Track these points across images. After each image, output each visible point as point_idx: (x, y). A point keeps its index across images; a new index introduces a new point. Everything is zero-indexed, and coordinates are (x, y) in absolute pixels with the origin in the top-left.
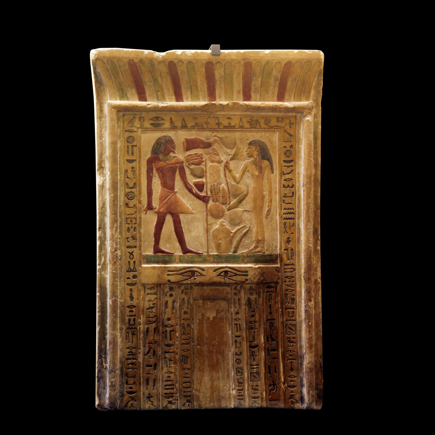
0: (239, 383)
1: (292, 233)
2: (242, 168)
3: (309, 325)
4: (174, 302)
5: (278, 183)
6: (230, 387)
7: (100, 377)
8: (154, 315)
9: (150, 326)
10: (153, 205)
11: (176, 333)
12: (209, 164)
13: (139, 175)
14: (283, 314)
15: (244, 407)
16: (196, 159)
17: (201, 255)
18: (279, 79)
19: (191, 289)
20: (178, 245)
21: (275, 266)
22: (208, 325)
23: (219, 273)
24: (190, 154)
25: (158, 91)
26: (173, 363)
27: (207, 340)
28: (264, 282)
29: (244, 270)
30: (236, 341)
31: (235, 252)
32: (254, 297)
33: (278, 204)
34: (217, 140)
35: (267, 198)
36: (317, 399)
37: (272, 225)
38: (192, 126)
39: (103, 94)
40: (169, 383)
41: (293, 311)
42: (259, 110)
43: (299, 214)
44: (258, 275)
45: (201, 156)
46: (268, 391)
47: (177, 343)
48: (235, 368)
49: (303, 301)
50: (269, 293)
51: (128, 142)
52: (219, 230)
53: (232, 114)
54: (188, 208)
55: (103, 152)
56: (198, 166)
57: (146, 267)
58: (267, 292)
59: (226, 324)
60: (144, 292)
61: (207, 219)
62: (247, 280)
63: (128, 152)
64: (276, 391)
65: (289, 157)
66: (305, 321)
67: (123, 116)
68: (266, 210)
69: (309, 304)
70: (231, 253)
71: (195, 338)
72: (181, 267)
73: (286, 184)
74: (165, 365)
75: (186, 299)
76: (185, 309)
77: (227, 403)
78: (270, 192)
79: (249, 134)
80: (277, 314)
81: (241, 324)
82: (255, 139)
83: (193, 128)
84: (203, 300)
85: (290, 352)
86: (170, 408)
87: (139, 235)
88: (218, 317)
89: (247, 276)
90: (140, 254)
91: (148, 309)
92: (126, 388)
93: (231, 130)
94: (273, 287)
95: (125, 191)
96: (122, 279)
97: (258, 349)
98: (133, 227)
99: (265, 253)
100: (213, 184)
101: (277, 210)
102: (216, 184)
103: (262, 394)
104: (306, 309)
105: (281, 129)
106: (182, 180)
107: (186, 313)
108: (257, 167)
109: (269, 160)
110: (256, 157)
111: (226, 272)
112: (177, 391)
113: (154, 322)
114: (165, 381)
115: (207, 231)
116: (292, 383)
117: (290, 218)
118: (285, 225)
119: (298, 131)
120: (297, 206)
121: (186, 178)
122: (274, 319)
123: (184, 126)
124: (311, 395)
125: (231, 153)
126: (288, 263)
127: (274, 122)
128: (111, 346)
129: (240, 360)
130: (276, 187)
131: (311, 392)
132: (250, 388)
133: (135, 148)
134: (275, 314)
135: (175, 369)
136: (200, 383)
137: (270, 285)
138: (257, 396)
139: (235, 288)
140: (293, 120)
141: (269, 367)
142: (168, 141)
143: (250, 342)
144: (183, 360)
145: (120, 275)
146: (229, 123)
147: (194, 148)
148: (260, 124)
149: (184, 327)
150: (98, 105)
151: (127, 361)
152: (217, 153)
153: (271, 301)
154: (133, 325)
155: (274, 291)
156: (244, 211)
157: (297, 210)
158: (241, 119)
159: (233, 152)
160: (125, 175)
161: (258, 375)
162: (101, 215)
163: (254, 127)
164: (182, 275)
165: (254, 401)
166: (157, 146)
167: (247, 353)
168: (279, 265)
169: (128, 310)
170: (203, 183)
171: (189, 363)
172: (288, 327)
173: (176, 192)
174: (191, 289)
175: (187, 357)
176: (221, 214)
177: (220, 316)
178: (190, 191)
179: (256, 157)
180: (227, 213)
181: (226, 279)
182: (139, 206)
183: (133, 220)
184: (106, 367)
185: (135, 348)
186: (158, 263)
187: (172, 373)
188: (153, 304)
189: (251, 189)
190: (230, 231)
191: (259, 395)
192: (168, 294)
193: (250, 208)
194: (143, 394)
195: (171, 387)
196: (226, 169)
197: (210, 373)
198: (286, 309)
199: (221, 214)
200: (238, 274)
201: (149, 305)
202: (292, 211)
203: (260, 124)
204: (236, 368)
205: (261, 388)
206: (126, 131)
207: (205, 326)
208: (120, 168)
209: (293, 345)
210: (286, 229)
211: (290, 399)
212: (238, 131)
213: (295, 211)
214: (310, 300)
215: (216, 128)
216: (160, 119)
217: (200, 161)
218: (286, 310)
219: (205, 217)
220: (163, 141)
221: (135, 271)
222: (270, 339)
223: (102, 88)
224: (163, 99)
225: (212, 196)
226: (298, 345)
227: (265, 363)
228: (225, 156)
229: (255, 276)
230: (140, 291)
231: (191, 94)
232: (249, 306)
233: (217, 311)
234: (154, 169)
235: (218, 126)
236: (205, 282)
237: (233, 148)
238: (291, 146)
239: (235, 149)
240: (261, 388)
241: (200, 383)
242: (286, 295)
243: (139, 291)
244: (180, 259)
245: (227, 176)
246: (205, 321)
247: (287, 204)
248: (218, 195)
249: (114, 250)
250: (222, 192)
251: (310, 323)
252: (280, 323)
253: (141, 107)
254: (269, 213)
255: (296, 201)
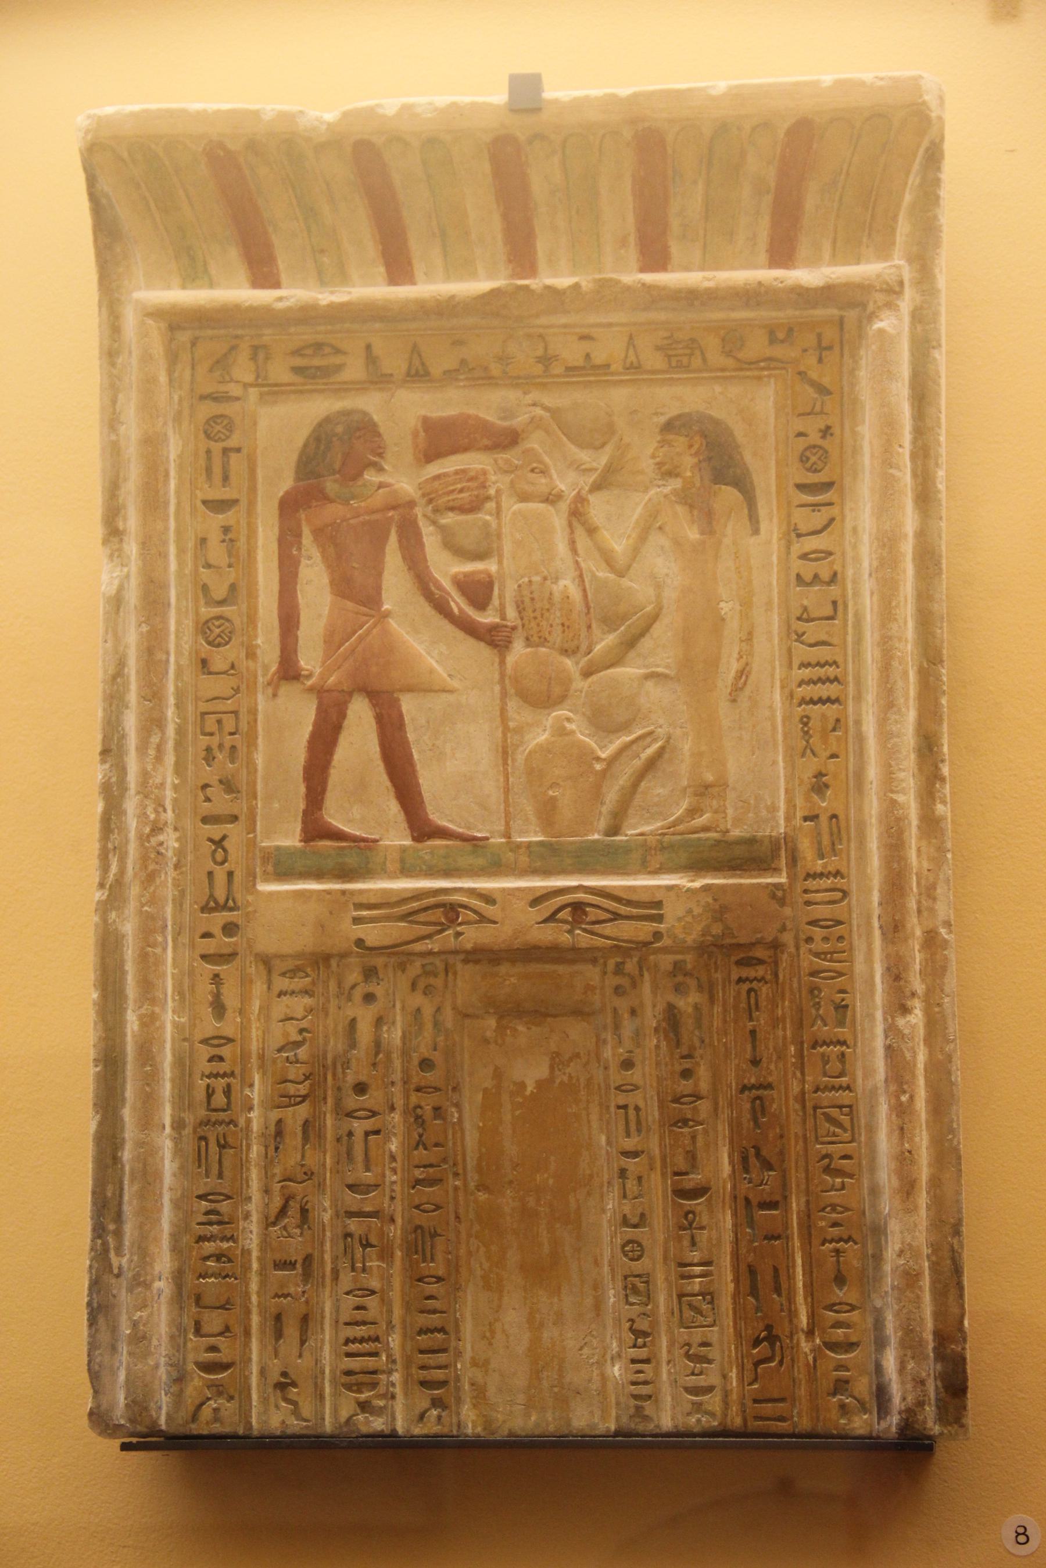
0: (638, 1333)
1: (834, 756)
2: (635, 517)
3: (901, 1104)
4: (379, 1022)
5: (775, 570)
6: (605, 1349)
7: (99, 1306)
8: (301, 1072)
9: (290, 1114)
10: (302, 663)
11: (388, 1140)
12: (512, 507)
13: (249, 554)
14: (803, 1064)
15: (657, 1426)
16: (461, 491)
17: (481, 843)
18: (773, 185)
19: (447, 974)
20: (393, 807)
21: (769, 880)
22: (518, 1113)
23: (552, 910)
24: (442, 471)
25: (322, 251)
26: (374, 1256)
27: (514, 1169)
28: (728, 941)
29: (645, 897)
30: (623, 1173)
31: (614, 830)
32: (690, 1000)
33: (777, 648)
34: (541, 418)
35: (733, 627)
36: (943, 1395)
37: (754, 726)
38: (445, 372)
39: (121, 270)
40: (360, 1331)
41: (843, 1055)
42: (696, 303)
43: (858, 683)
44: (700, 915)
45: (479, 480)
46: (749, 1366)
47: (394, 1178)
48: (620, 1277)
49: (879, 1015)
50: (745, 987)
51: (208, 436)
52: (549, 752)
53: (598, 320)
54: (432, 671)
55: (121, 475)
56: (469, 517)
57: (271, 894)
58: (740, 980)
59: (587, 1109)
60: (265, 986)
61: (503, 711)
62: (657, 935)
63: (209, 470)
64: (781, 1362)
65: (816, 471)
66: (887, 1091)
67: (193, 344)
68: (733, 674)
69: (901, 1022)
70: (596, 837)
71: (471, 1163)
72: (405, 890)
73: (808, 570)
74: (344, 1264)
75: (428, 1011)
76: (425, 1051)
77: (592, 1413)
78: (746, 604)
79: (663, 393)
80: (781, 1065)
81: (641, 1104)
82: (687, 410)
83: (450, 376)
84: (501, 1017)
85: (834, 1210)
86: (364, 1430)
87: (249, 773)
88: (558, 1081)
89: (661, 922)
90: (252, 843)
91: (279, 1050)
92: (196, 1349)
93: (592, 378)
94: (761, 962)
95: (197, 613)
96: (185, 939)
97: (709, 1200)
98: (227, 746)
99: (728, 831)
100: (526, 580)
101: (774, 668)
102: (537, 579)
103: (725, 1377)
104: (888, 1042)
105: (784, 368)
106: (410, 569)
107: (426, 1064)
108: (695, 512)
109: (742, 484)
110: (689, 474)
111: (578, 907)
112: (394, 1362)
113: (304, 1098)
114: (346, 1324)
115: (505, 753)
116: (839, 1331)
117: (824, 697)
118: (806, 724)
119: (852, 372)
120: (850, 652)
121: (426, 561)
122: (769, 1086)
123: (417, 374)
124: (909, 1378)
125: (595, 465)
126: (819, 869)
127: (757, 346)
128: (135, 1187)
129: (640, 1245)
130: (770, 584)
131: (911, 1365)
132: (678, 1352)
133: (234, 457)
134: (772, 1067)
135: (386, 1279)
136: (488, 1334)
137: (751, 954)
138: (703, 1384)
139: (619, 970)
140: (830, 334)
141: (752, 1271)
142: (359, 429)
143: (676, 1174)
144: (416, 1246)
145: (174, 924)
146: (588, 356)
147: (454, 451)
148: (702, 353)
149: (421, 1117)
150: (104, 309)
151: (201, 1248)
152: (541, 466)
153: (755, 1014)
154: (224, 1110)
155: (769, 977)
156: (648, 677)
157: (850, 666)
158: (631, 337)
159: (603, 460)
160: (196, 557)
161: (711, 1302)
162: (111, 706)
163: (681, 367)
164: (410, 922)
165: (693, 1403)
166: (318, 447)
167: (665, 1216)
168: (783, 879)
169: (205, 1052)
170: (490, 576)
171: (440, 1257)
172: (824, 1114)
173: (387, 615)
174: (447, 974)
175: (434, 1235)
176: (557, 690)
177: (565, 1078)
178: (441, 608)
179: (689, 474)
180: (580, 684)
181: (578, 931)
182: (248, 668)
183: (224, 721)
184: (120, 1268)
185: (228, 1197)
186: (319, 875)
187: (373, 1292)
188: (301, 1031)
189: (670, 595)
190: (593, 752)
191: (714, 1379)
192: (358, 994)
193: (667, 667)
194: (263, 1372)
195: (366, 1347)
196: (575, 523)
197: (525, 1298)
198: (815, 1045)
199: (557, 690)
200: (622, 913)
201: (286, 1034)
202: (831, 671)
203: (702, 353)
204: (626, 1277)
205: (723, 1352)
206: (203, 398)
207: (507, 1118)
208: (179, 532)
209: (843, 1183)
210: (811, 741)
211: (834, 1394)
212: (622, 381)
213: (845, 673)
214: (905, 1010)
215: (539, 377)
216: (327, 350)
217: (477, 496)
218: (814, 1047)
219: (498, 702)
220: (340, 429)
221: (231, 909)
222: (753, 1160)
223: (118, 250)
224: (343, 277)
225: (523, 626)
226: (866, 1183)
227: (736, 1255)
228: (572, 476)
229: (689, 919)
230: (251, 982)
231: (445, 256)
232: (672, 1035)
233: (553, 1059)
234: (306, 532)
235: (547, 368)
236: (496, 947)
237: (603, 445)
238: (826, 432)
239: (609, 449)
240: (723, 1352)
241: (488, 1334)
242: (813, 990)
243: (245, 982)
244: (402, 861)
245: (580, 551)
246: (505, 1098)
247: (811, 645)
248: (548, 620)
249: (147, 830)
250: (561, 609)
251: (904, 1098)
252: (791, 1102)
253: (252, 309)
254: (745, 683)
255: (846, 633)
